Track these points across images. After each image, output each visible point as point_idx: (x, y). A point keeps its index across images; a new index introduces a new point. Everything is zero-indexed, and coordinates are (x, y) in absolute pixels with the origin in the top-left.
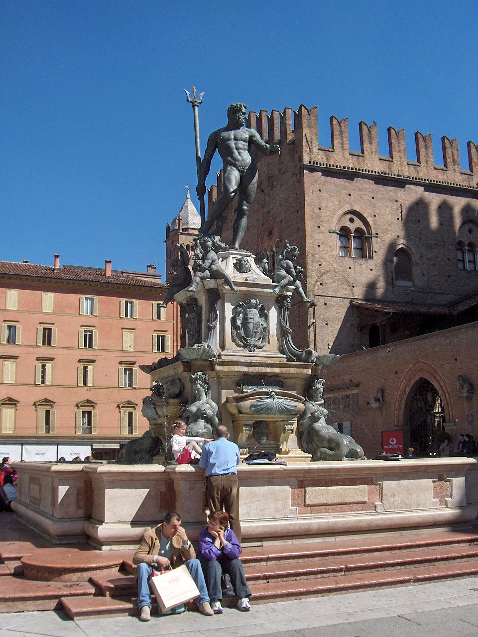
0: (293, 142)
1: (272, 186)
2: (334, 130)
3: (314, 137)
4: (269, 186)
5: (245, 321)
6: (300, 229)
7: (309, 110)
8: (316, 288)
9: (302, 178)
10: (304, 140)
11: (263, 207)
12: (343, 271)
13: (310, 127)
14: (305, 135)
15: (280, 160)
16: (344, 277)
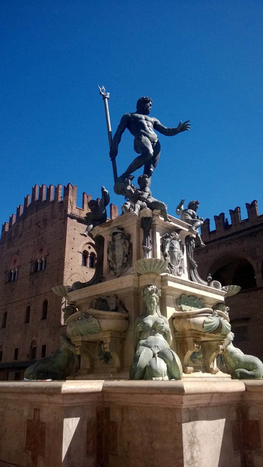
0: (62, 202)
1: (46, 225)
2: (85, 199)
3: (74, 201)
4: (43, 224)
5: (172, 248)
6: (62, 249)
7: (73, 186)
8: (68, 282)
9: (66, 221)
10: (69, 202)
11: (39, 235)
12: (84, 274)
13: (73, 196)
14: (70, 199)
15: (52, 211)
16: (83, 278)
